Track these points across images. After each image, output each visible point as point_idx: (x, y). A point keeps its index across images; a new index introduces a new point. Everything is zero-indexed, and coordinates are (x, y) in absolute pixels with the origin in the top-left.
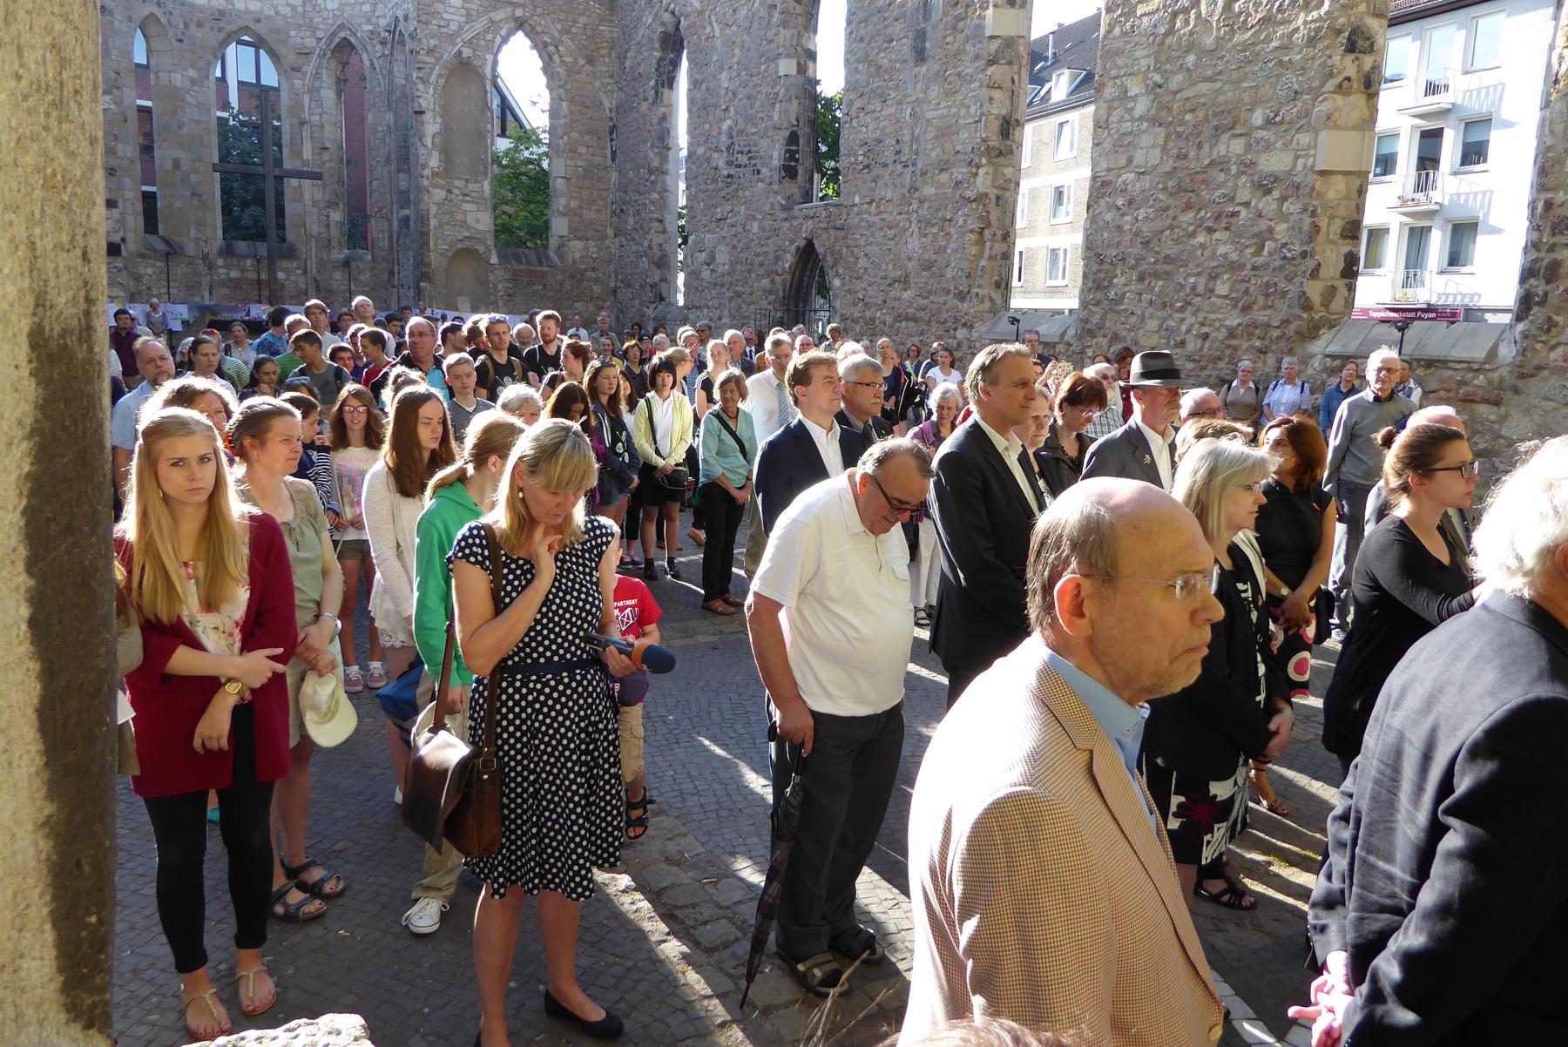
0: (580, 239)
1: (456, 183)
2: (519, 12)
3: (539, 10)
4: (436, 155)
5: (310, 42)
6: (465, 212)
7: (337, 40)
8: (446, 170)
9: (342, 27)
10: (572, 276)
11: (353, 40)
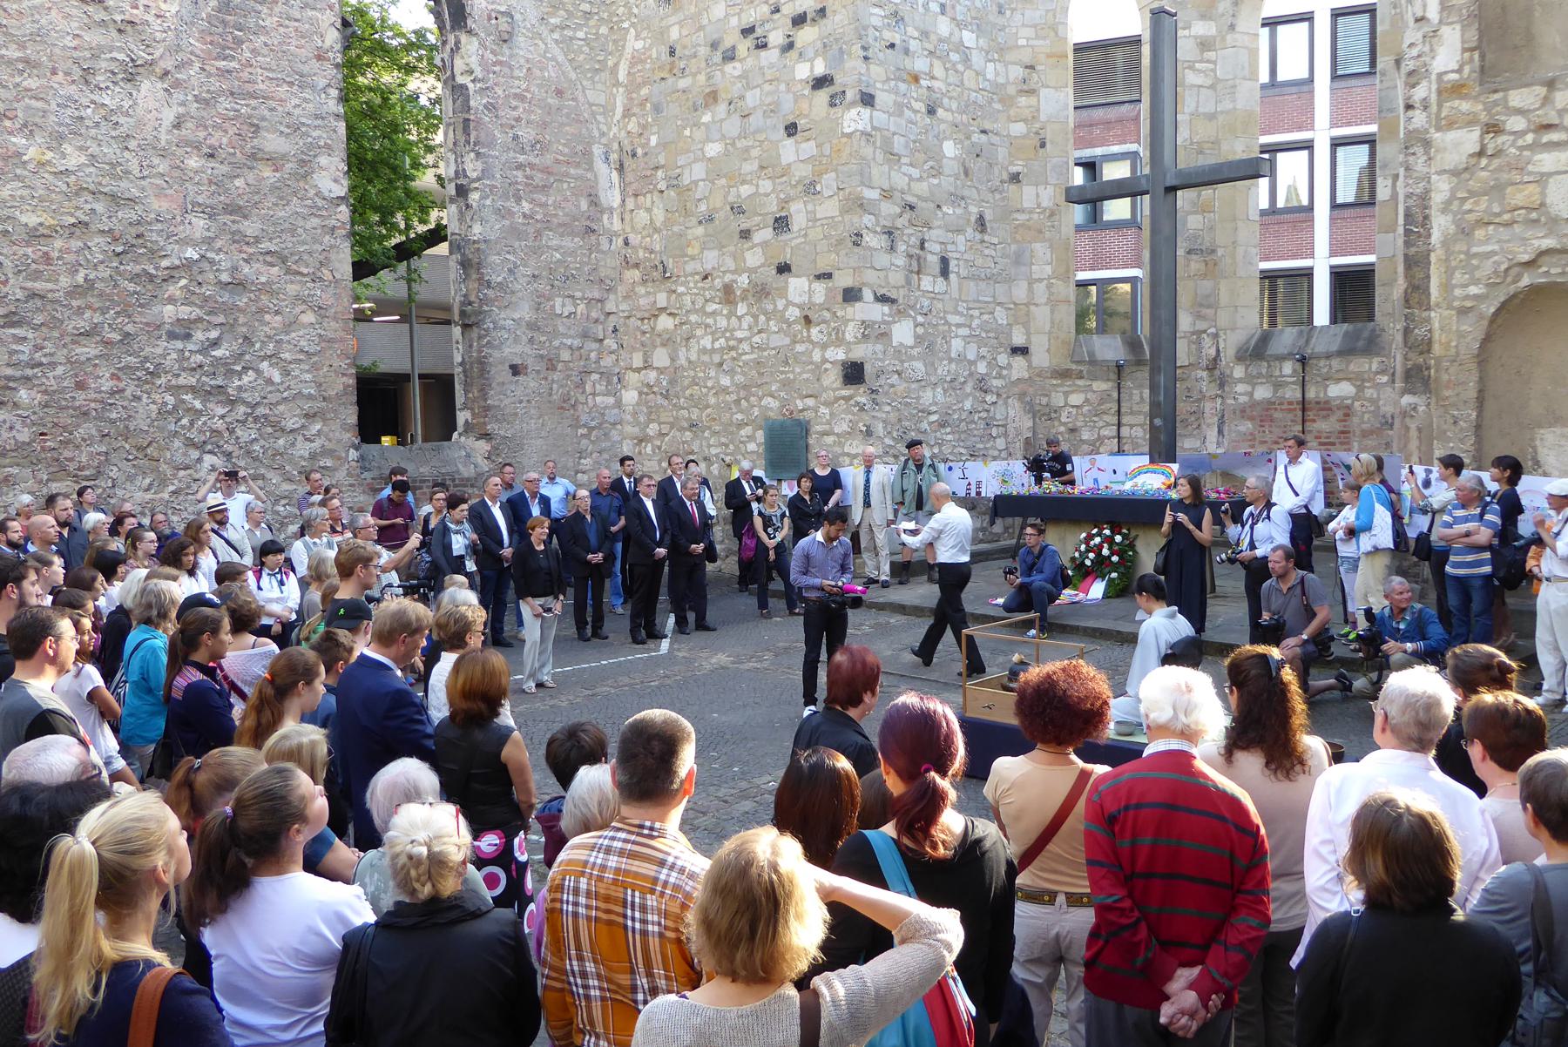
1: (1517, 98)
6: (1542, 179)
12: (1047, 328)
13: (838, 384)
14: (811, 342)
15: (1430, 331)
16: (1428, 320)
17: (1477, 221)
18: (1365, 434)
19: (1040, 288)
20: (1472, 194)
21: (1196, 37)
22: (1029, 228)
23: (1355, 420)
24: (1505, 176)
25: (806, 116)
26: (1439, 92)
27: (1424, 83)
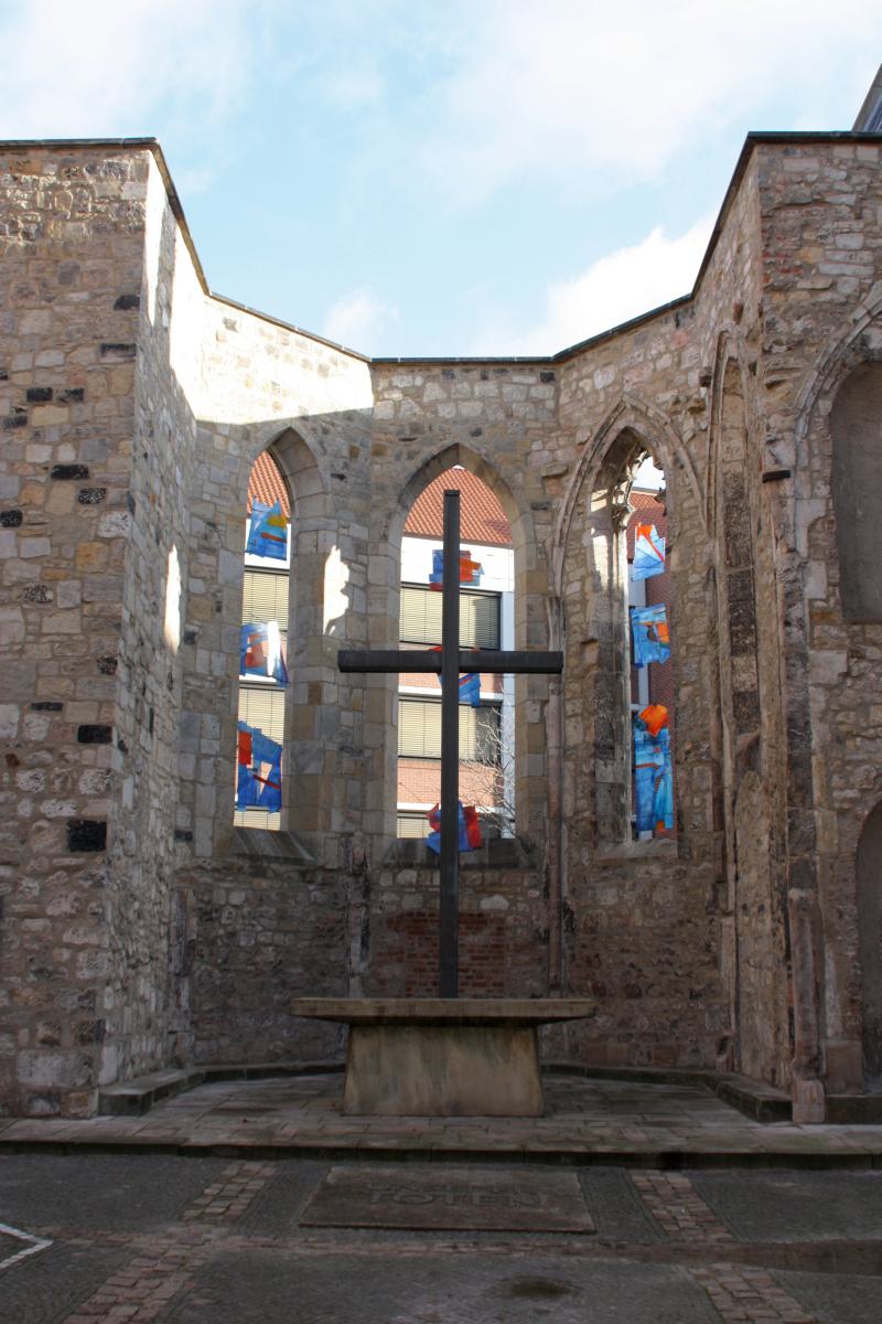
7: (612, 436)
9: (619, 410)
11: (641, 428)
12: (212, 812)
13: (58, 849)
14: (18, 791)
15: (814, 828)
16: (812, 818)
17: (848, 733)
18: (519, 949)
19: (207, 765)
20: (843, 708)
21: (353, 539)
22: (200, 696)
23: (509, 934)
24: (868, 697)
25: (39, 508)
26: (811, 617)
27: (799, 605)
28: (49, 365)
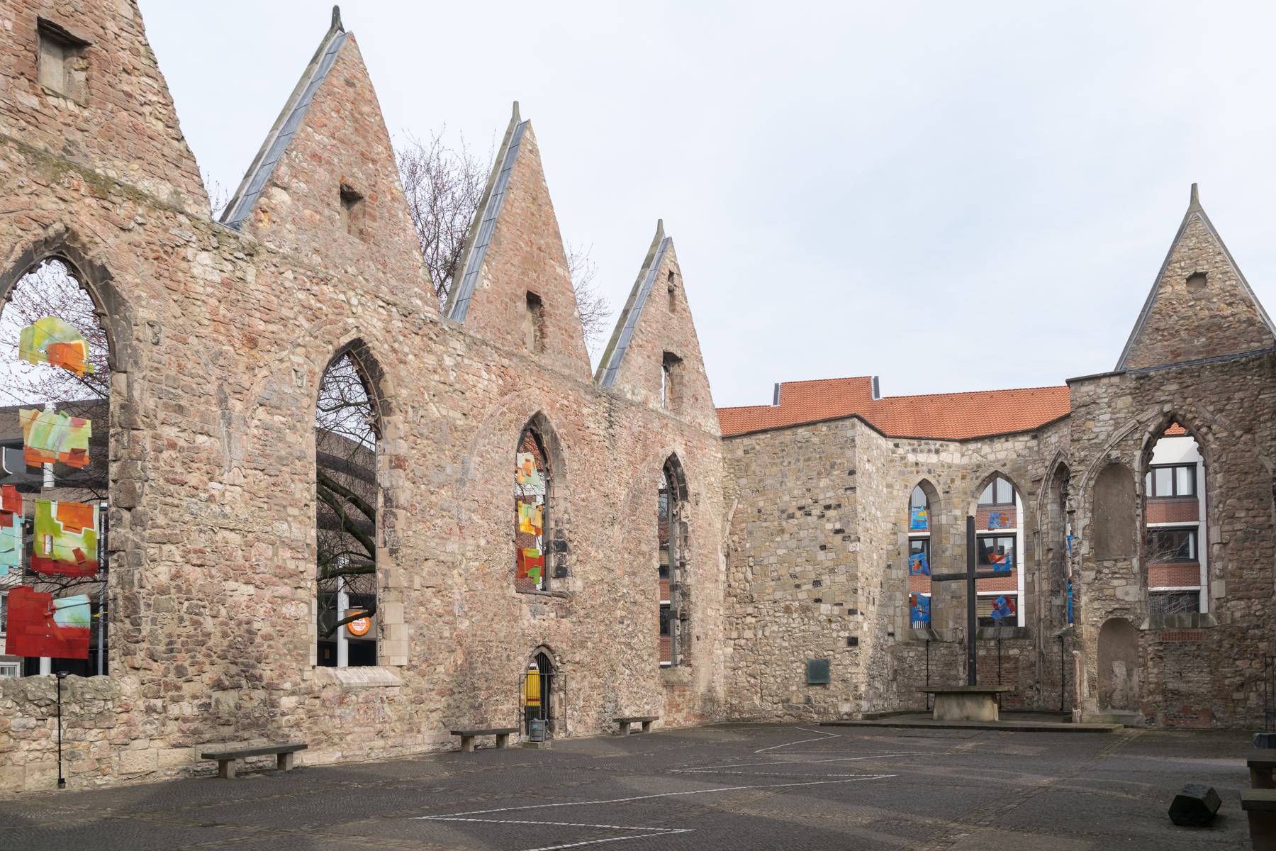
0: (1240, 599)
1: (1106, 564)
2: (1167, 408)
3: (1190, 400)
4: (1086, 544)
5: (1042, 471)
6: (1114, 588)
8: (1096, 555)
9: (1059, 454)
10: (1232, 635)
28: (828, 497)
